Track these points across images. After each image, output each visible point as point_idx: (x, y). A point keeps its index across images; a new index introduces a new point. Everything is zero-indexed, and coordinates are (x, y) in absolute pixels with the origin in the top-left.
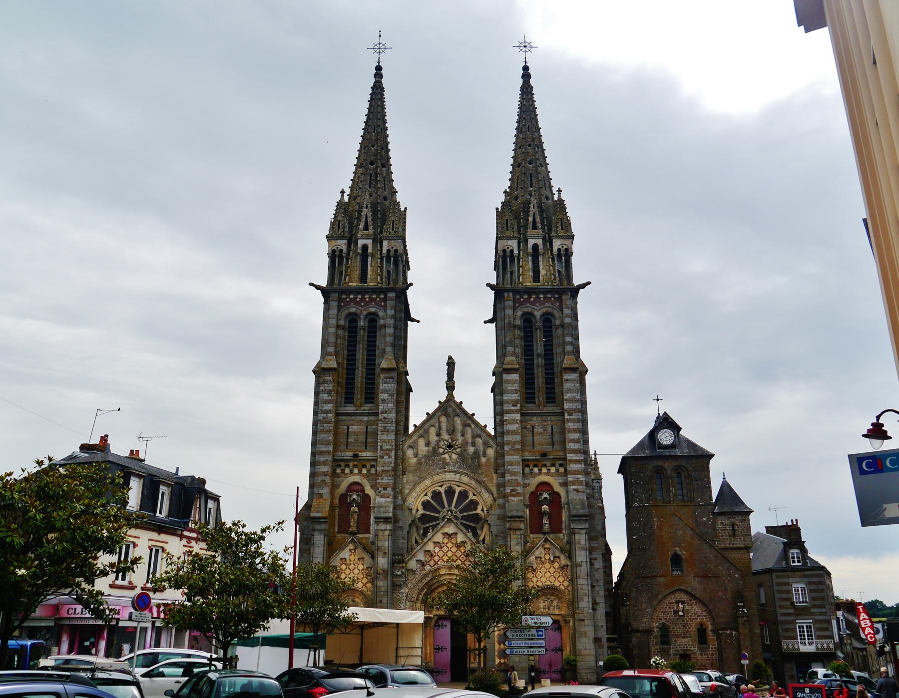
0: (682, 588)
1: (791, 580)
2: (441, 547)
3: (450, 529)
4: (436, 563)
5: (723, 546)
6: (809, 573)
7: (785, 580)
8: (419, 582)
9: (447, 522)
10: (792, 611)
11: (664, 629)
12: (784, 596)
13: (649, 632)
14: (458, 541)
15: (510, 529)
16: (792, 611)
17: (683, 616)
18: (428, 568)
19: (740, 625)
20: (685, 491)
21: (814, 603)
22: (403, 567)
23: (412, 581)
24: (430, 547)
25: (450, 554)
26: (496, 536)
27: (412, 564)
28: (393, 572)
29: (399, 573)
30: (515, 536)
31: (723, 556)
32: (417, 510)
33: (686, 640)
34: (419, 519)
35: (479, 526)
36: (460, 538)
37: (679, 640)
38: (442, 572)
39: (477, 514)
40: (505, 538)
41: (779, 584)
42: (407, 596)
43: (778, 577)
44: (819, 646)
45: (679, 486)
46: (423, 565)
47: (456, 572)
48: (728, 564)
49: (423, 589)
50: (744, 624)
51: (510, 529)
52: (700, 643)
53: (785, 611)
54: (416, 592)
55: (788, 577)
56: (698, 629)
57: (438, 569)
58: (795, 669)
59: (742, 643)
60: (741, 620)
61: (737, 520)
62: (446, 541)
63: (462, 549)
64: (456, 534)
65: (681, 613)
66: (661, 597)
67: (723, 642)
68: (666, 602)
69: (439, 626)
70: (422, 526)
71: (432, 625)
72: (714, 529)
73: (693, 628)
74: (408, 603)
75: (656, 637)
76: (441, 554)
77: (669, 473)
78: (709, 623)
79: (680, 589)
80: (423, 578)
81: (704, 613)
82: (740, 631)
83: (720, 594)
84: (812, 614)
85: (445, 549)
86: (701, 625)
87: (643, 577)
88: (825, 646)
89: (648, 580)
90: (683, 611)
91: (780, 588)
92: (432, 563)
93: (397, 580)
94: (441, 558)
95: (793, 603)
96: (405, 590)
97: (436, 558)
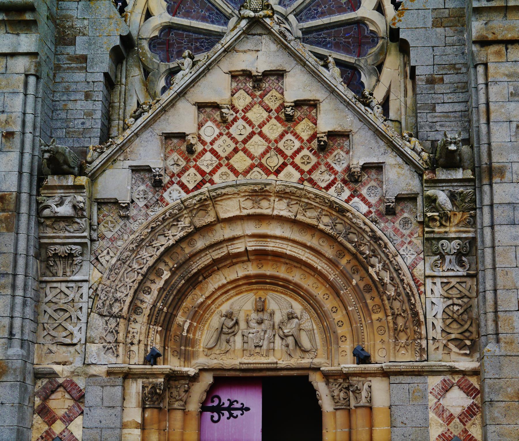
2: (225, 123)
3: (260, 57)
4: (205, 178)
8: (140, 244)
9: (247, 33)
14: (290, 97)
15: (484, 43)
18: (174, 195)
22: (79, 188)
23: (117, 238)
24: (183, 119)
25: (257, 146)
26: (431, 81)
27: (117, 182)
28: (40, 207)
29: (65, 210)
30: (506, 68)
32: (148, 15)
34: (153, 42)
35: (366, 62)
36: (297, 86)
38: (229, 208)
39: (360, 22)
40: (464, 88)
42: (95, 296)
46: (158, 184)
47: (281, 208)
49: (154, 270)
51: (484, 43)
54: (132, 279)
57: (214, 199)
62: (242, 100)
63: (304, 129)
64: (279, 74)
69: (219, 409)
70: (164, 67)
71: (194, 406)
74: (97, 321)
76: (223, 147)
80: (155, 230)
85: (240, 129)
92: (191, 178)
93: (60, 238)
94: (224, 161)
96: (89, 273)
97: (207, 162)
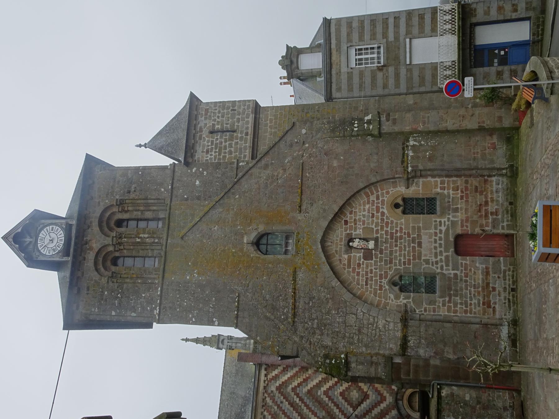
0: (319, 236)
1: (344, 69)
5: (248, 153)
6: (333, 41)
7: (344, 78)
10: (391, 70)
11: (402, 285)
12: (368, 80)
13: (406, 319)
16: (391, 70)
17: (376, 240)
19: (397, 129)
20: (148, 215)
21: (379, 36)
31: (267, 153)
33: (425, 239)
37: (426, 251)
41: (350, 89)
43: (339, 89)
44: (449, 26)
45: (142, 224)
48: (282, 144)
50: (395, 122)
52: (432, 211)
53: (391, 81)
55: (339, 73)
56: (404, 212)
58: (486, 69)
59: (432, 128)
60: (387, 127)
61: (205, 124)
65: (371, 245)
66: (335, 283)
67: (430, 165)
68: (346, 274)
72: (217, 166)
73: (404, 222)
75: (419, 304)
77: (108, 241)
78: (392, 191)
79: (323, 241)
81: (373, 198)
82: (408, 129)
83: (335, 164)
84: (397, 38)
86: (397, 206)
87: (294, 315)
88: (448, 17)
89: (301, 305)
90: (366, 240)
91: (356, 86)
95: (380, 69)
